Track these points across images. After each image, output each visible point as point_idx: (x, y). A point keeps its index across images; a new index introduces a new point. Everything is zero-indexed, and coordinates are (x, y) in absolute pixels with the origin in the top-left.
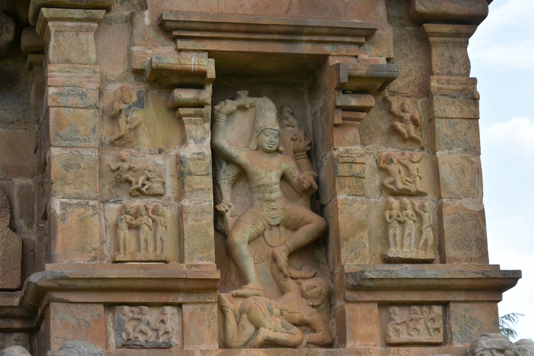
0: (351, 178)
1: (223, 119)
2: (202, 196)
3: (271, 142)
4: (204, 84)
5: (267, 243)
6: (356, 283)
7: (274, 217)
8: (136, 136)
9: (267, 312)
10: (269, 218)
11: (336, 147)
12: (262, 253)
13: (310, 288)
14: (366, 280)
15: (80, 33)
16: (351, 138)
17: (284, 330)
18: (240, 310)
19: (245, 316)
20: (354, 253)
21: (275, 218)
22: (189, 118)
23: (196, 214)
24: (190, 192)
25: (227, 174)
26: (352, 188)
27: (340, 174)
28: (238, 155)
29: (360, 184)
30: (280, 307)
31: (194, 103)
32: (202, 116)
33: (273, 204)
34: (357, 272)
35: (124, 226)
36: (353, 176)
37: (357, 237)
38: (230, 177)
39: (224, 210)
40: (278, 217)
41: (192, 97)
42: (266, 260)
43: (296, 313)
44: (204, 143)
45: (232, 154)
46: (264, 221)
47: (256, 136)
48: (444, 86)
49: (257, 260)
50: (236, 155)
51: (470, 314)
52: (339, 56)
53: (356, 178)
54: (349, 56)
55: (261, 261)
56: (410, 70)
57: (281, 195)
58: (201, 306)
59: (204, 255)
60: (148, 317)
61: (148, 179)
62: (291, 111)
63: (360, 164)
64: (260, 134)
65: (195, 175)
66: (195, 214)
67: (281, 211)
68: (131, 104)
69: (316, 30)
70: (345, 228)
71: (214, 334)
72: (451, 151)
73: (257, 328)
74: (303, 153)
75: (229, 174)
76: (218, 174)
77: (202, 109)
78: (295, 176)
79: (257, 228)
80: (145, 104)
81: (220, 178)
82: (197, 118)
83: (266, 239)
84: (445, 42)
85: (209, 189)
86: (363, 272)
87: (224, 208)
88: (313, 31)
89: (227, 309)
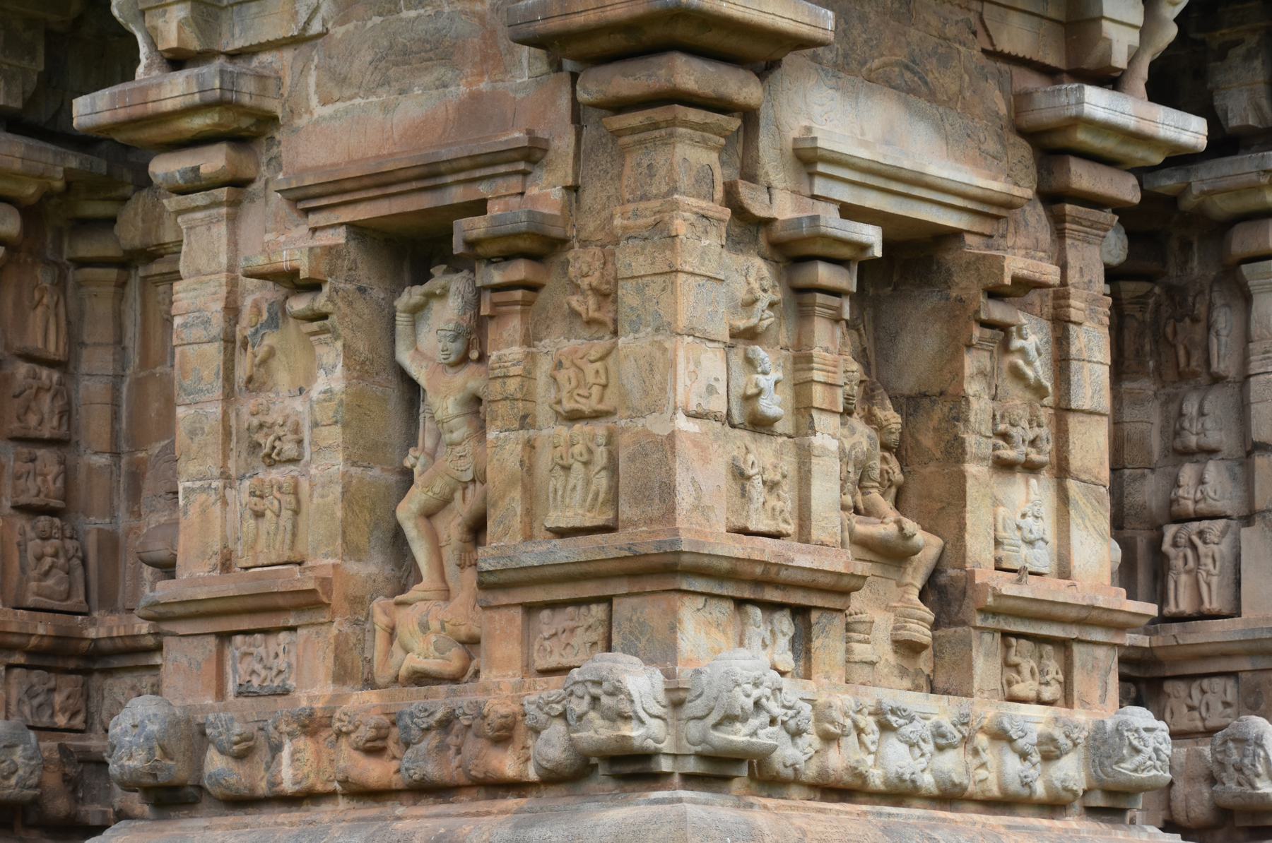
8: (269, 373)
9: (417, 628)
15: (212, 226)
17: (437, 654)
22: (317, 337)
33: (459, 448)
35: (248, 514)
37: (507, 500)
46: (447, 478)
48: (631, 223)
51: (638, 614)
52: (498, 197)
54: (511, 195)
56: (608, 198)
60: (262, 650)
61: (279, 439)
68: (259, 326)
69: (455, 165)
72: (637, 336)
77: (325, 322)
80: (280, 321)
84: (640, 142)
88: (454, 166)
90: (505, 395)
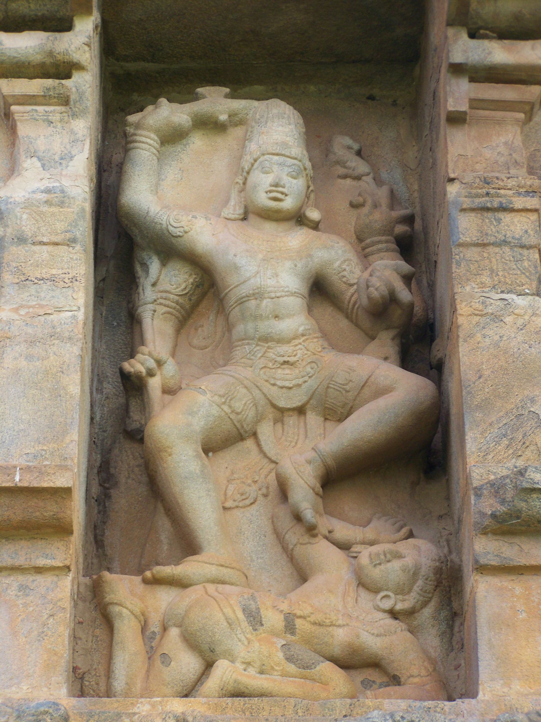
0: (497, 250)
1: (147, 143)
2: (53, 297)
3: (277, 185)
4: (73, 16)
5: (265, 456)
6: (503, 509)
7: (287, 384)
9: (241, 615)
10: (271, 387)
11: (454, 173)
12: (249, 481)
13: (382, 557)
14: (535, 496)
16: (499, 153)
17: (292, 668)
18: (164, 620)
19: (174, 632)
20: (507, 443)
21: (290, 388)
22: (29, 108)
23: (32, 342)
24: (16, 287)
25: (162, 289)
26: (500, 273)
27: (463, 239)
28: (186, 229)
29: (526, 264)
30: (285, 607)
31: (42, 65)
32: (65, 101)
34: (507, 477)
36: (505, 242)
38: (172, 296)
39: (143, 370)
40: (299, 385)
41: (33, 45)
42: (261, 498)
43: (335, 625)
44: (67, 167)
45: (171, 229)
46: (256, 392)
47: (241, 182)
49: (234, 501)
50: (182, 229)
53: (512, 248)
55: (248, 502)
57: (307, 327)
58: (21, 579)
59: (45, 448)
62: (356, 147)
63: (523, 214)
64: (248, 173)
65: (34, 244)
66: (25, 341)
67: (308, 369)
70: (480, 377)
71: (55, 658)
73: (209, 665)
74: (384, 238)
75: (168, 287)
76: (139, 294)
77: (63, 82)
78: (352, 282)
79: (230, 407)
81: (141, 303)
82: (52, 108)
83: (263, 443)
85: (74, 279)
86: (521, 473)
87: (142, 364)
89: (116, 609)
90: (501, 237)
